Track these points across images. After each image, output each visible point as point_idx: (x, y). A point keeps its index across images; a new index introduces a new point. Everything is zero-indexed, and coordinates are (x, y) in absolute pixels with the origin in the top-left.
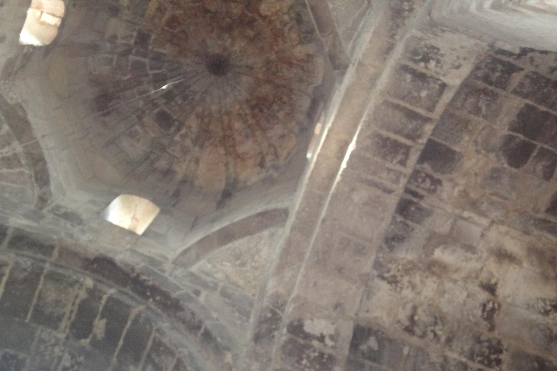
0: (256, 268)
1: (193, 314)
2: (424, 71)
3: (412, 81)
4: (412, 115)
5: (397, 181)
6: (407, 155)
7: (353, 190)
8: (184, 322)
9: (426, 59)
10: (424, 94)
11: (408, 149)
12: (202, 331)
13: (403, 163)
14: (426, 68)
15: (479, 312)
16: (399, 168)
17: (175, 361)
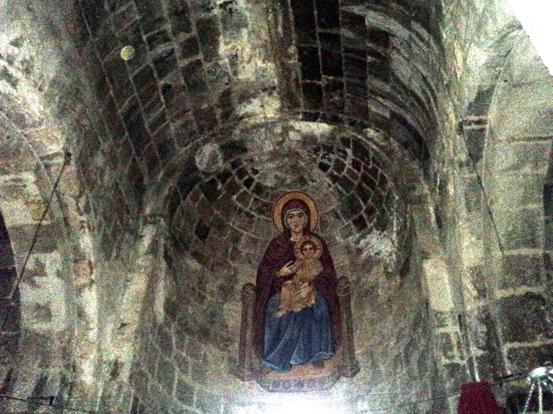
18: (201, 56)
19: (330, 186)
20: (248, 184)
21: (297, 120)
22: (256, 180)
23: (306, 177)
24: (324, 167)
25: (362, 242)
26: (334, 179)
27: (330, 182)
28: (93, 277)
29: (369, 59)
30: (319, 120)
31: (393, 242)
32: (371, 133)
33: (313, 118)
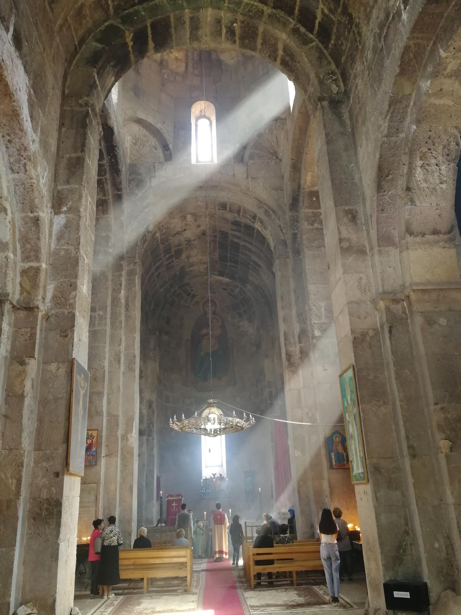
0: (138, 152)
1: (120, 183)
2: (257, 220)
3: (252, 215)
4: (239, 212)
5: (211, 209)
6: (223, 210)
7: (202, 202)
8: (114, 179)
9: (261, 223)
10: (248, 216)
11: (226, 210)
12: (119, 193)
13: (219, 209)
14: (258, 221)
15: (175, 232)
16: (217, 209)
17: (104, 198)
18: (174, 259)
19: (227, 296)
20: (188, 295)
21: (215, 275)
22: (192, 293)
23: (216, 291)
24: (225, 289)
25: (241, 324)
26: (230, 294)
27: (227, 295)
28: (143, 375)
29: (251, 266)
30: (225, 276)
31: (254, 330)
32: (249, 287)
33: (222, 274)
